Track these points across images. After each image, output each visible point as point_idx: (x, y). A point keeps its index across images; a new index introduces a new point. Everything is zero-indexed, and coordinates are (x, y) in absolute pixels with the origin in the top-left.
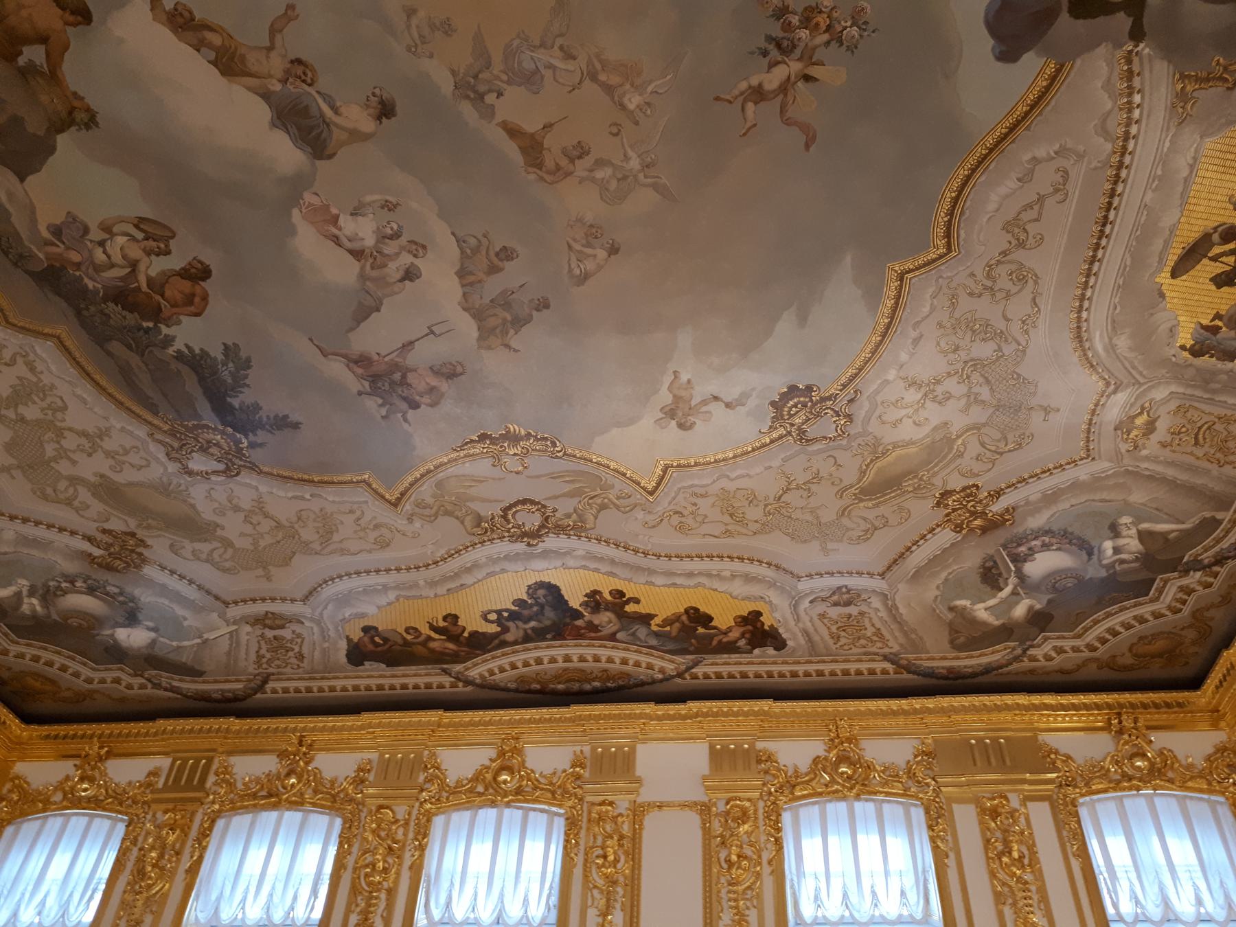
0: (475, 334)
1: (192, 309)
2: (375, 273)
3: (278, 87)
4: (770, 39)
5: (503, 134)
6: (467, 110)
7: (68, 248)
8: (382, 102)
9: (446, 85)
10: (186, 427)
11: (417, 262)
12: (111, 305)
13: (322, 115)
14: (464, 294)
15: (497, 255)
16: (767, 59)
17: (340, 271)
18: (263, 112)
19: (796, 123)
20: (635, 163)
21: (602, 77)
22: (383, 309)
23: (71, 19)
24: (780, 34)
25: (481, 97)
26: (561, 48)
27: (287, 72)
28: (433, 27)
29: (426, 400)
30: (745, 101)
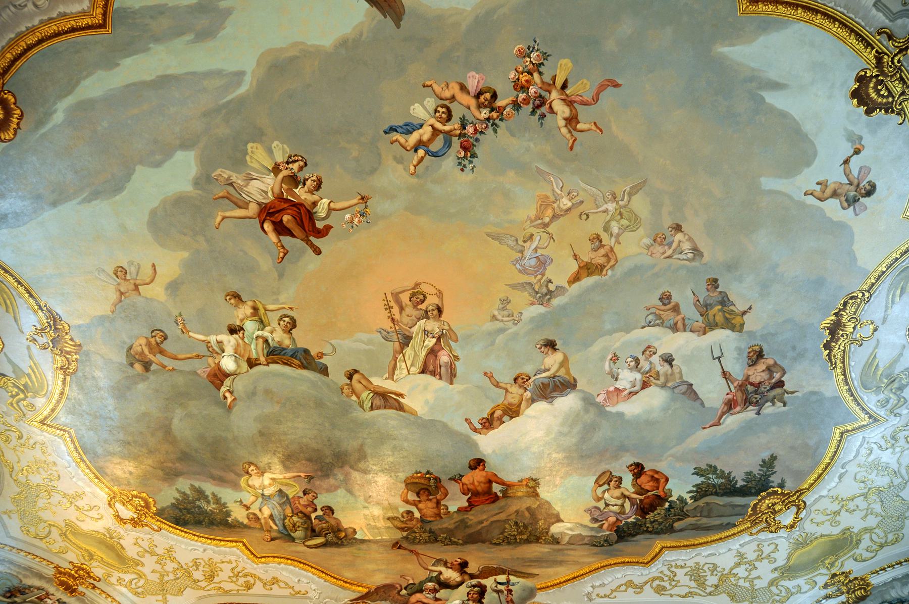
0: (728, 332)
1: (662, 481)
2: (662, 379)
3: (528, 394)
4: (533, 112)
5: (576, 285)
6: (556, 302)
7: (606, 520)
8: (546, 346)
9: (539, 309)
10: (751, 515)
11: (659, 353)
12: (647, 516)
13: (549, 378)
14: (691, 331)
15: (664, 304)
16: (547, 114)
17: (654, 399)
18: (541, 406)
19: (598, 94)
20: (611, 207)
21: (547, 220)
22: (691, 381)
23: (481, 467)
24: (531, 105)
25: (550, 292)
26: (525, 242)
27: (520, 387)
28: (504, 309)
29: (777, 376)
30: (575, 129)
